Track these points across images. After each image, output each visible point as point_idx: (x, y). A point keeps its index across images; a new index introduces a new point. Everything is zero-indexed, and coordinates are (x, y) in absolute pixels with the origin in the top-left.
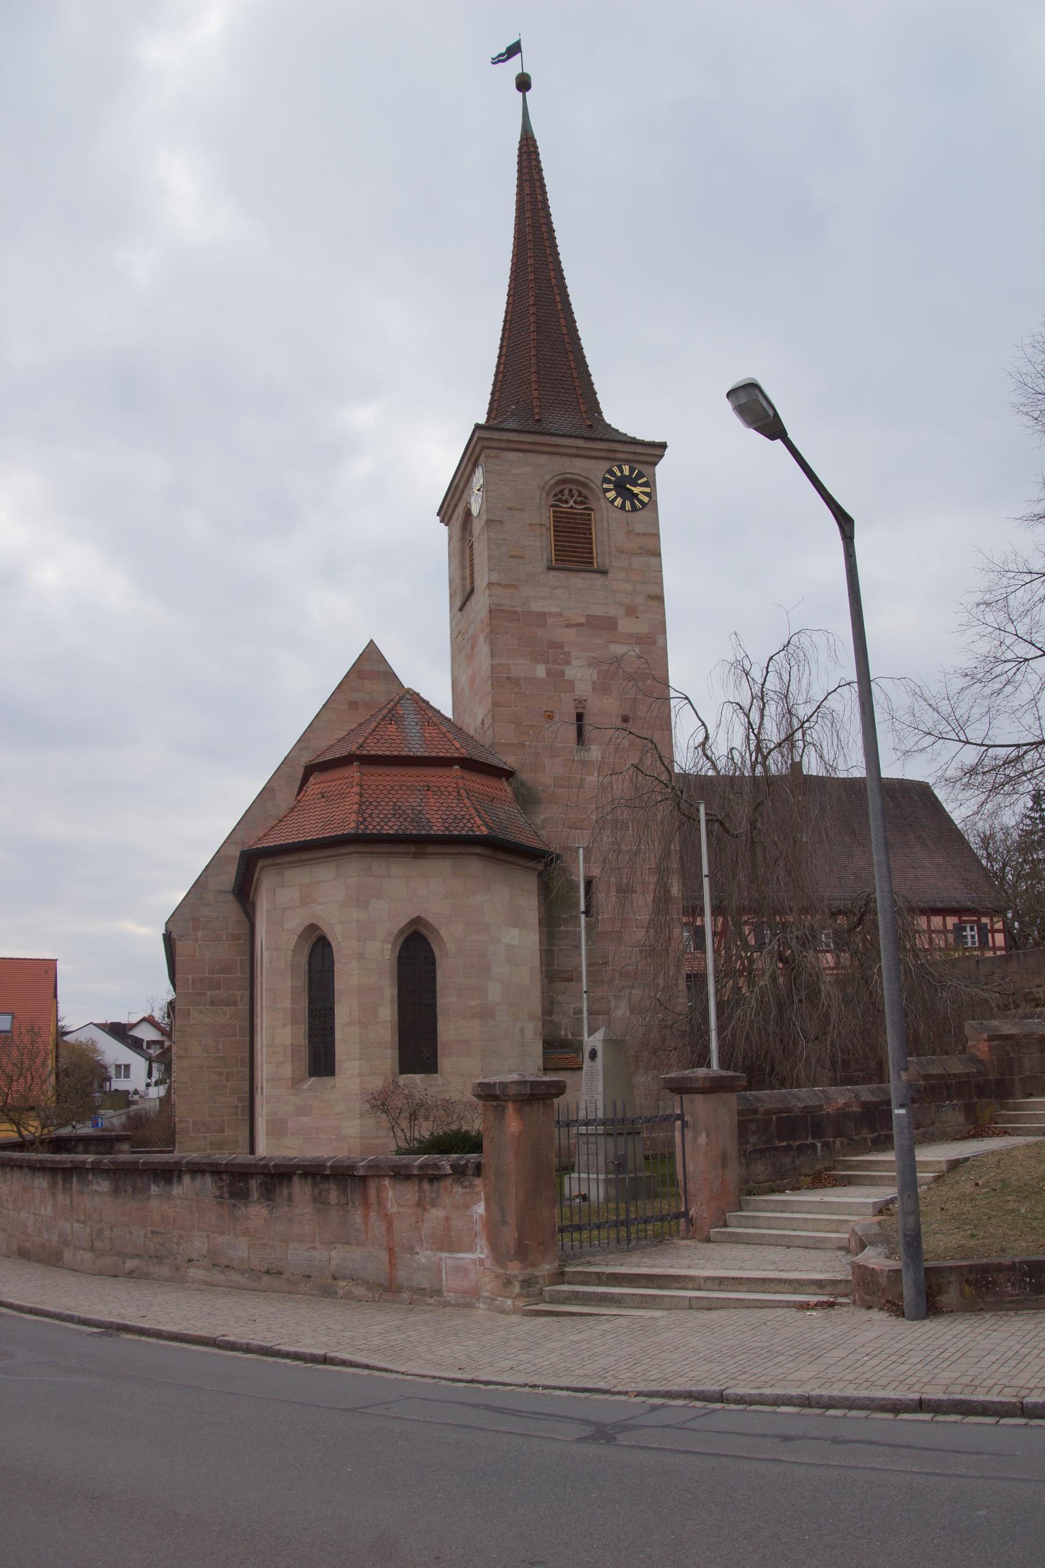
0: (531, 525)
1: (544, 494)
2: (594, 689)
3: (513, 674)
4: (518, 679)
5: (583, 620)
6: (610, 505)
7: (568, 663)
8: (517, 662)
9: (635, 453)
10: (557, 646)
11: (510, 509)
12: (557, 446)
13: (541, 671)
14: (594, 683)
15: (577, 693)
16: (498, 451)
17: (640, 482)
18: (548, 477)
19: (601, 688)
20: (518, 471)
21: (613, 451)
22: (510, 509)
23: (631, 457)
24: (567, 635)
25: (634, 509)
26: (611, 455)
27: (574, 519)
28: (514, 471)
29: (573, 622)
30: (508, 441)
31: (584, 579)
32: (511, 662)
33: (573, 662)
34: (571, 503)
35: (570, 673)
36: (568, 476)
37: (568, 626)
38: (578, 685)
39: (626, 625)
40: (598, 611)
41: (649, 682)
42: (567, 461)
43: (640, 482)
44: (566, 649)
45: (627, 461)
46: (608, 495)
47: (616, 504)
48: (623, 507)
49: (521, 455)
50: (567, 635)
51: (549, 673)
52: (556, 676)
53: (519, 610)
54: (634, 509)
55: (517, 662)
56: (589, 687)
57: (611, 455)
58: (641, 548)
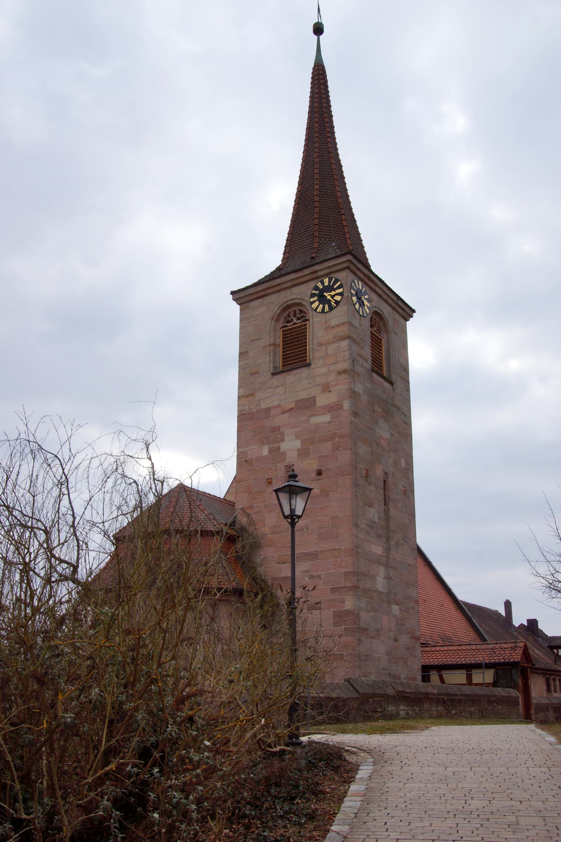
0: (265, 347)
1: (273, 322)
2: (298, 455)
3: (249, 457)
4: (251, 460)
5: (293, 405)
6: (314, 313)
7: (282, 440)
8: (252, 448)
9: (329, 267)
10: (276, 429)
11: (252, 341)
12: (279, 285)
13: (265, 451)
14: (299, 450)
15: (287, 461)
16: (247, 304)
17: (335, 287)
18: (276, 308)
19: (303, 453)
20: (258, 313)
21: (315, 272)
22: (252, 341)
23: (328, 271)
24: (281, 420)
25: (331, 308)
26: (314, 276)
27: (295, 332)
28: (255, 314)
29: (287, 409)
30: (250, 295)
31: (295, 374)
32: (248, 449)
33: (285, 439)
34: (295, 321)
35: (284, 446)
36: (288, 303)
37: (283, 413)
38: (288, 455)
39: (322, 400)
40: (303, 395)
41: (337, 439)
42: (288, 292)
43: (335, 287)
44: (281, 430)
45: (326, 275)
46: (313, 306)
47: (318, 311)
48: (323, 311)
49: (260, 300)
50: (281, 420)
51: (270, 451)
52: (276, 452)
53: (254, 410)
54: (331, 308)
55: (252, 448)
56: (295, 455)
57: (314, 276)
58: (334, 337)
